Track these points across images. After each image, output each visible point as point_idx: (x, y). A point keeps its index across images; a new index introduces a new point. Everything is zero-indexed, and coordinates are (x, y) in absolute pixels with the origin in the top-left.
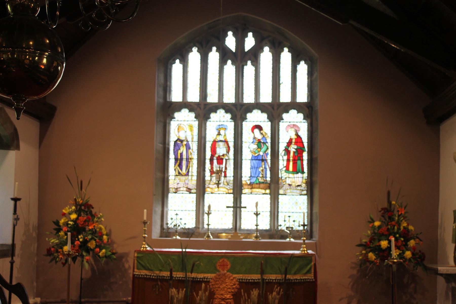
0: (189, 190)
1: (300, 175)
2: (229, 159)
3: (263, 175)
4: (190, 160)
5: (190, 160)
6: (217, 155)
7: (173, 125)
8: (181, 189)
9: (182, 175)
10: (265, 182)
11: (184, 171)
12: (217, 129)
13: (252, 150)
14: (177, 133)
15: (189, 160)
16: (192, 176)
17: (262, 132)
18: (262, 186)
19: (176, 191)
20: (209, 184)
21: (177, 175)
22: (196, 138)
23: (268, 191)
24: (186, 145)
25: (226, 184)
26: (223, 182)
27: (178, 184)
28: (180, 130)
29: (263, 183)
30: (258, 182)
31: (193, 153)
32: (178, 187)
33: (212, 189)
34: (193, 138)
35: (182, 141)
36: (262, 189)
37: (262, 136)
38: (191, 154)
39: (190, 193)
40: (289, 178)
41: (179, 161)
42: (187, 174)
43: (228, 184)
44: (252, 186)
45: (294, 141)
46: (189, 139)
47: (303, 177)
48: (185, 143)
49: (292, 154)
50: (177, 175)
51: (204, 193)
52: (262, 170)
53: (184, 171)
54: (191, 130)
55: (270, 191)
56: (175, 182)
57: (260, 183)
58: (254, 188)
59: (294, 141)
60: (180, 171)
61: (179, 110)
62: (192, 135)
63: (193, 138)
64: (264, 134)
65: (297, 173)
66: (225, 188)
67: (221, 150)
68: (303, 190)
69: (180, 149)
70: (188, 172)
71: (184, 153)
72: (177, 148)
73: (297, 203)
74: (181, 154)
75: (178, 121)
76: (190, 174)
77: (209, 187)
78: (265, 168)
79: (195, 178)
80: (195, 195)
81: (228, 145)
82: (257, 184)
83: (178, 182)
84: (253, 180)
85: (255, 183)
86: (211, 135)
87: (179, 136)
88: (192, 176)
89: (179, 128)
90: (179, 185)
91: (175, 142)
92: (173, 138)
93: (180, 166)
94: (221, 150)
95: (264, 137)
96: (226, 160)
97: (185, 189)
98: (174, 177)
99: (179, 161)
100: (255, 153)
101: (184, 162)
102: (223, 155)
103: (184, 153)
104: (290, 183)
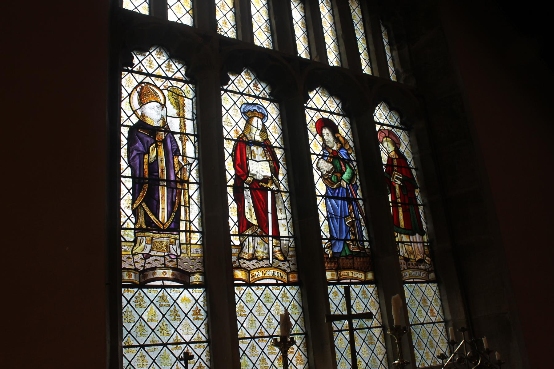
0: (183, 279)
1: (417, 237)
2: (279, 191)
3: (354, 235)
4: (179, 186)
5: (179, 186)
6: (249, 179)
7: (128, 82)
8: (159, 273)
9: (159, 230)
10: (362, 253)
11: (163, 215)
12: (244, 113)
13: (325, 173)
14: (136, 105)
15: (177, 186)
16: (188, 232)
17: (337, 135)
18: (358, 261)
19: (144, 280)
20: (239, 258)
21: (141, 229)
22: (190, 128)
23: (370, 276)
24: (164, 141)
25: (281, 258)
26: (274, 252)
27: (147, 256)
28: (146, 99)
29: (358, 254)
30: (348, 253)
31: (187, 167)
32: (148, 266)
33: (247, 271)
34: (183, 126)
35: (153, 130)
36: (358, 270)
37: (340, 145)
38: (182, 168)
39: (187, 285)
40: (403, 243)
41: (146, 187)
42: (174, 228)
43: (286, 259)
44: (338, 262)
45: (395, 163)
46: (174, 125)
47: (423, 242)
48: (162, 135)
49: (398, 191)
50: (141, 229)
51: (231, 283)
52: (352, 223)
53: (163, 215)
54: (179, 106)
55: (374, 275)
56: (138, 249)
57: (353, 255)
58: (344, 269)
59: (395, 163)
60: (153, 217)
61: (143, 49)
62: (181, 116)
63: (183, 126)
64: (341, 139)
65: (414, 234)
66: (278, 268)
67: (259, 168)
68: (429, 272)
69: (148, 153)
70: (177, 220)
71: (162, 164)
72: (139, 145)
73: (425, 301)
74: (153, 166)
75: (140, 73)
76: (182, 227)
77: (239, 268)
78: (357, 219)
79: (196, 238)
80: (198, 293)
81: (273, 155)
82: (347, 257)
83: (147, 251)
84: (339, 247)
85: (343, 254)
86: (232, 123)
87: (143, 115)
88: (188, 232)
89: (144, 94)
90: (150, 260)
91: (133, 129)
92: (128, 116)
93: (152, 202)
94: (259, 168)
95: (342, 147)
96: (273, 191)
97: (169, 274)
98: (132, 233)
99: (147, 184)
100: (333, 183)
101: (163, 191)
102: (265, 180)
103: (162, 164)
104: (406, 255)
